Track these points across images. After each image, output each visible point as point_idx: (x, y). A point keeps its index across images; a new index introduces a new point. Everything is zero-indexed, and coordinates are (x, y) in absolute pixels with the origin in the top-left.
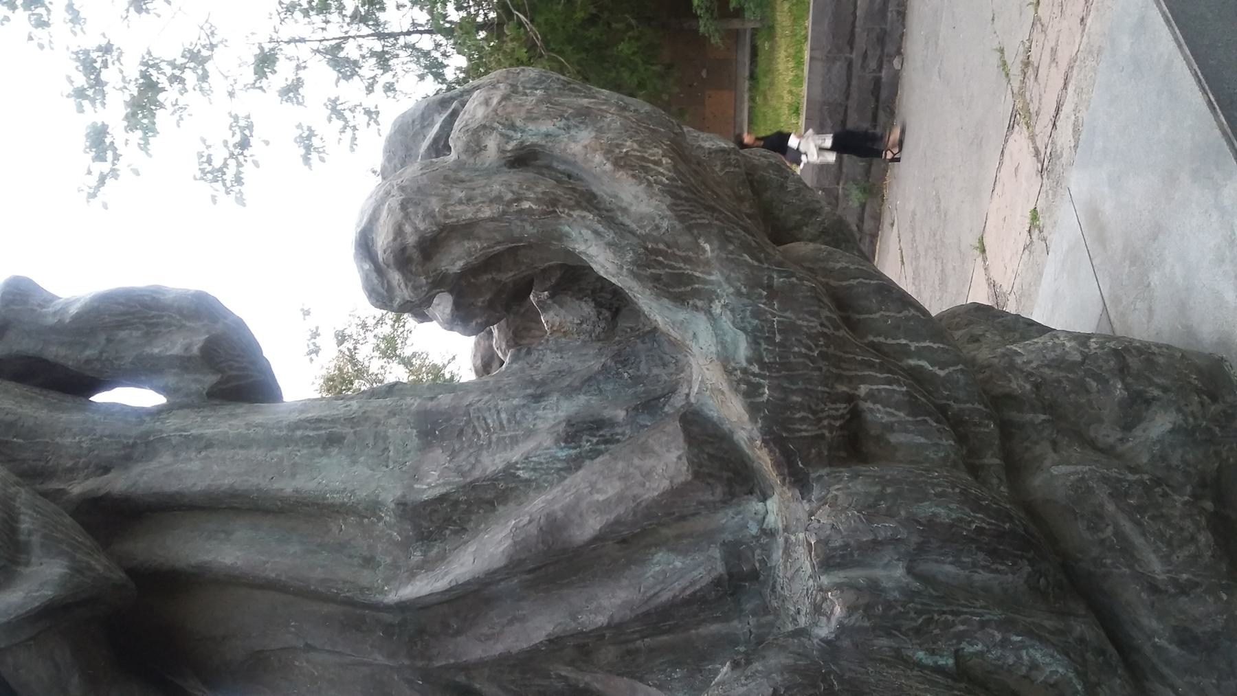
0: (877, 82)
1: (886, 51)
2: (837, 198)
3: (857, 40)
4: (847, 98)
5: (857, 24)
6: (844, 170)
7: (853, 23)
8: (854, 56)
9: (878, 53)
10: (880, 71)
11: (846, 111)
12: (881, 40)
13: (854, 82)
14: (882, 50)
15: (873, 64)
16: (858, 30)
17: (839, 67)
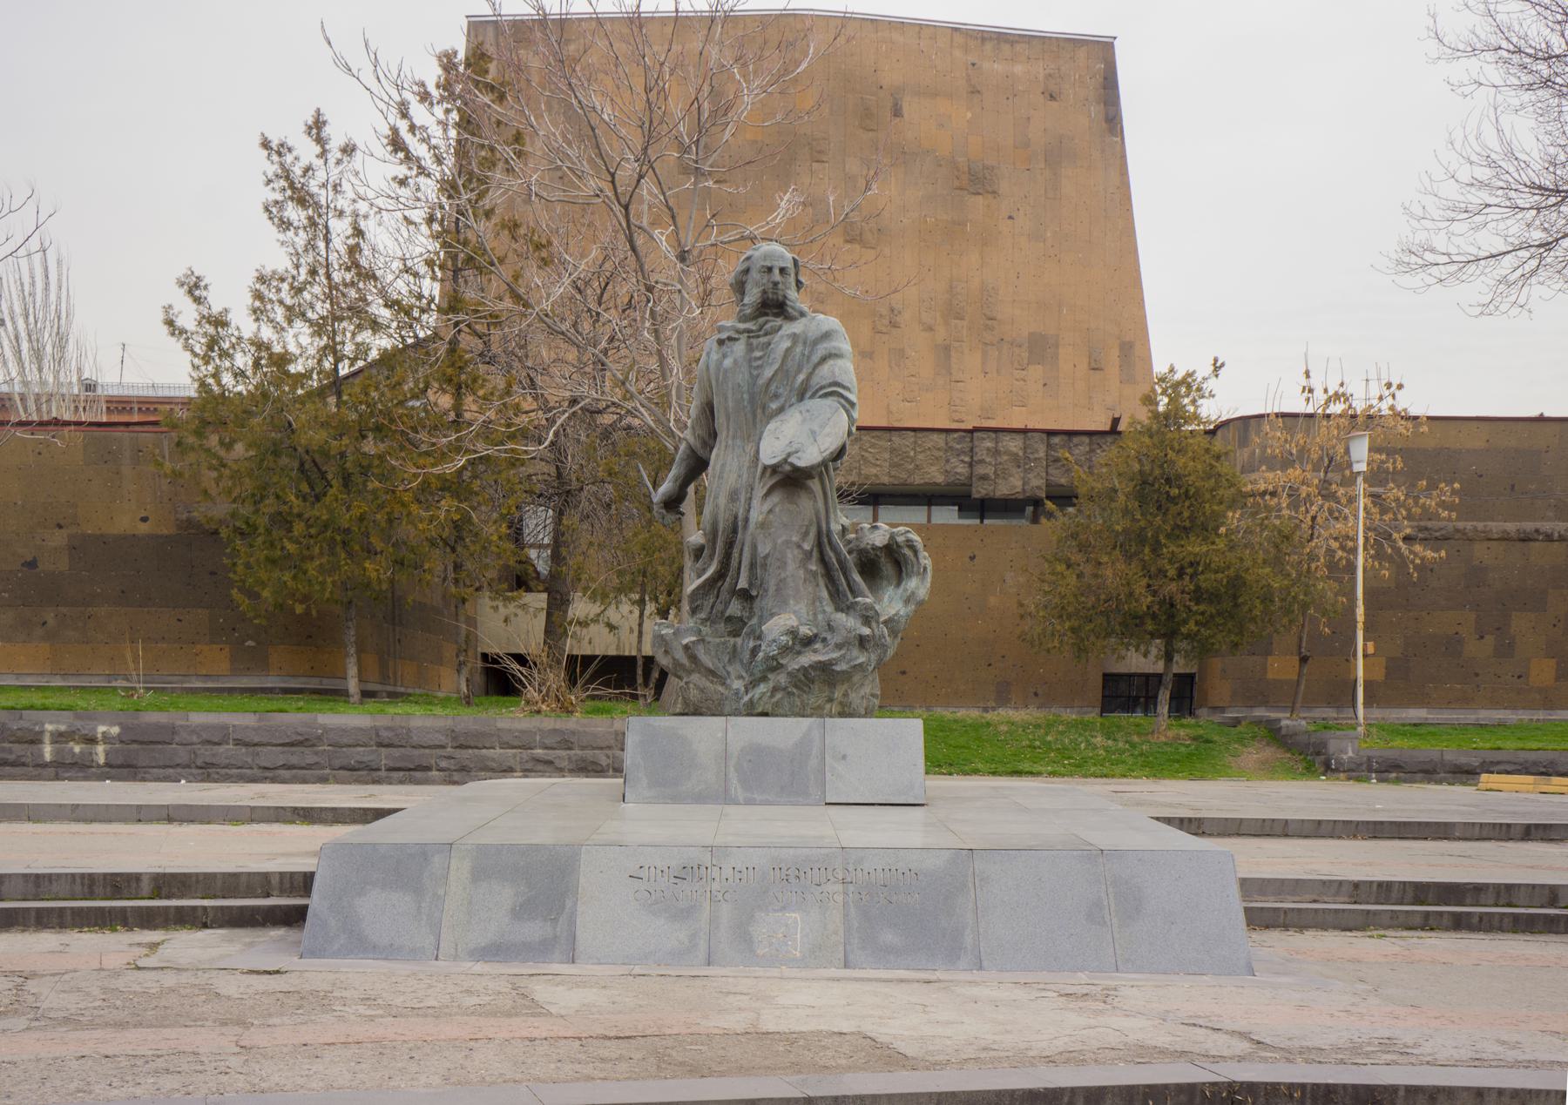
0: (428, 769)
1: (454, 773)
2: (313, 745)
3: (464, 751)
4: (413, 747)
5: (476, 751)
6: (344, 749)
7: (477, 748)
8: (449, 749)
9: (453, 767)
10: (438, 770)
11: (401, 746)
12: (463, 769)
13: (427, 751)
14: (455, 770)
15: (443, 764)
16: (470, 751)
17: (441, 739)
